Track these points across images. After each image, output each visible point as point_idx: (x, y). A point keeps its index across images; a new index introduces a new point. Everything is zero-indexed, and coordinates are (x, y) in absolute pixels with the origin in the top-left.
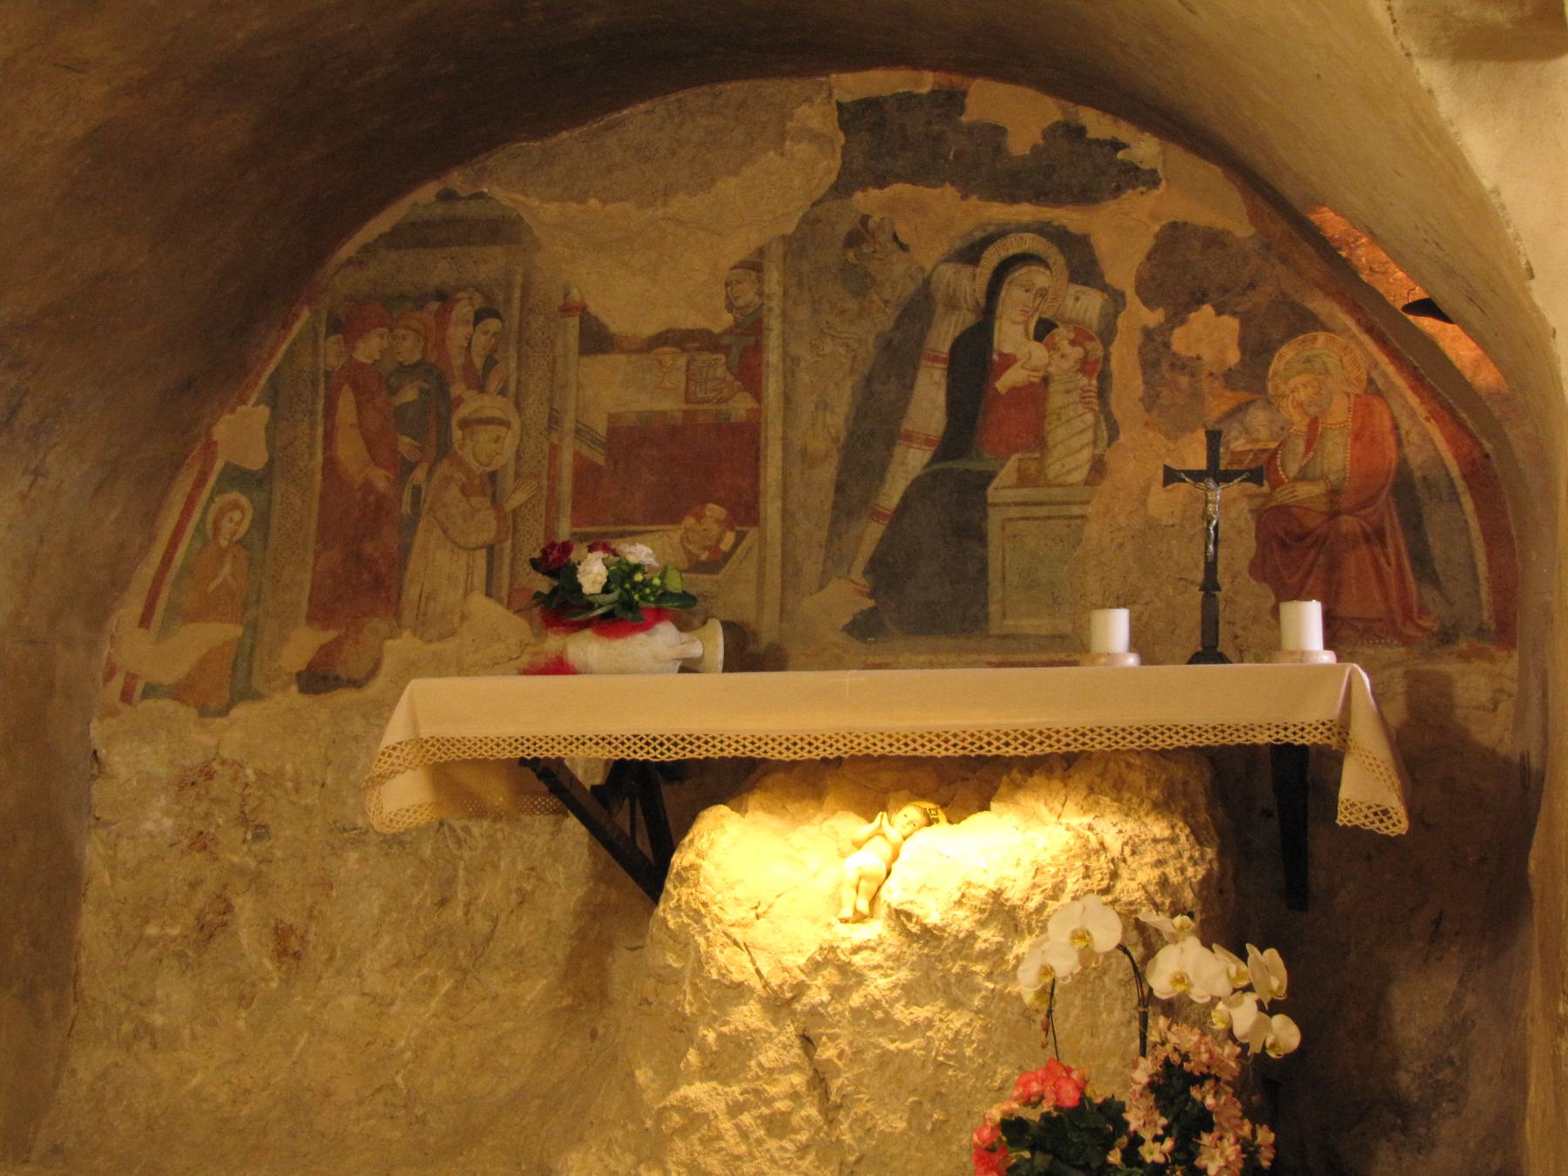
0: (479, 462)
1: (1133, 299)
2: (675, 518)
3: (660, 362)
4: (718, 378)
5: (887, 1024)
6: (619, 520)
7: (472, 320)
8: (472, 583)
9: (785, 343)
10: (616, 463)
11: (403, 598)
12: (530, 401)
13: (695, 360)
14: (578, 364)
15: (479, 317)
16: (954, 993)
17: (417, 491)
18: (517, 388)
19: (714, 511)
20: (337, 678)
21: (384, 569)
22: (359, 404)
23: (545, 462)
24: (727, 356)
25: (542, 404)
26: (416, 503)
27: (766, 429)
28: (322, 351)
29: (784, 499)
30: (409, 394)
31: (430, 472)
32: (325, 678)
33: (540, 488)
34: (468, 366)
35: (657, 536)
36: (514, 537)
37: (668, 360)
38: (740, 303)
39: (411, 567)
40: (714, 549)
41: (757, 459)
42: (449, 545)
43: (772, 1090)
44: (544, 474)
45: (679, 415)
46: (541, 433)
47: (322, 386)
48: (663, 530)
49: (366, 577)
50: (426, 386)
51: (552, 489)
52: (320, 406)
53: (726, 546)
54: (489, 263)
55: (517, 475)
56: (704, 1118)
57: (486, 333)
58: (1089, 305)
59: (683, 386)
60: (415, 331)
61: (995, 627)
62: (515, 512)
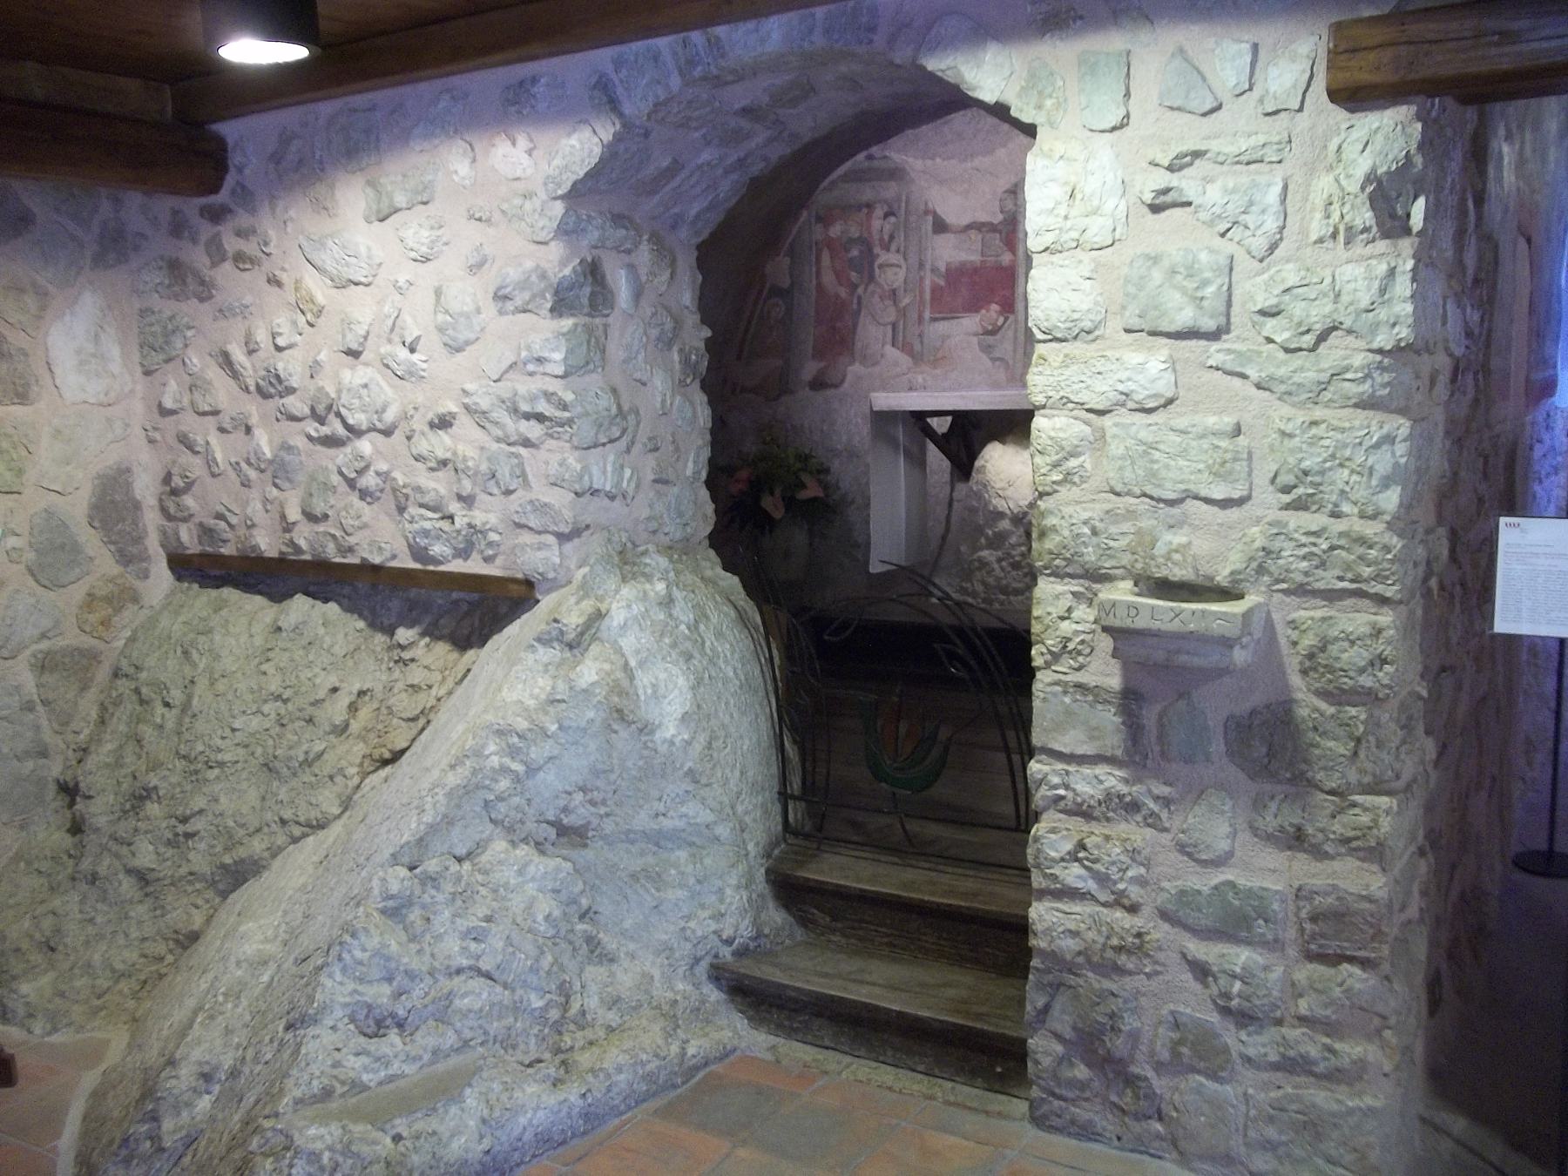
2: (977, 311)
6: (951, 311)
15: (886, 216)
19: (995, 307)
26: (859, 303)
30: (855, 253)
34: (881, 239)
43: (1014, 553)
53: (1000, 323)
54: (890, 190)
55: (905, 291)
56: (987, 564)
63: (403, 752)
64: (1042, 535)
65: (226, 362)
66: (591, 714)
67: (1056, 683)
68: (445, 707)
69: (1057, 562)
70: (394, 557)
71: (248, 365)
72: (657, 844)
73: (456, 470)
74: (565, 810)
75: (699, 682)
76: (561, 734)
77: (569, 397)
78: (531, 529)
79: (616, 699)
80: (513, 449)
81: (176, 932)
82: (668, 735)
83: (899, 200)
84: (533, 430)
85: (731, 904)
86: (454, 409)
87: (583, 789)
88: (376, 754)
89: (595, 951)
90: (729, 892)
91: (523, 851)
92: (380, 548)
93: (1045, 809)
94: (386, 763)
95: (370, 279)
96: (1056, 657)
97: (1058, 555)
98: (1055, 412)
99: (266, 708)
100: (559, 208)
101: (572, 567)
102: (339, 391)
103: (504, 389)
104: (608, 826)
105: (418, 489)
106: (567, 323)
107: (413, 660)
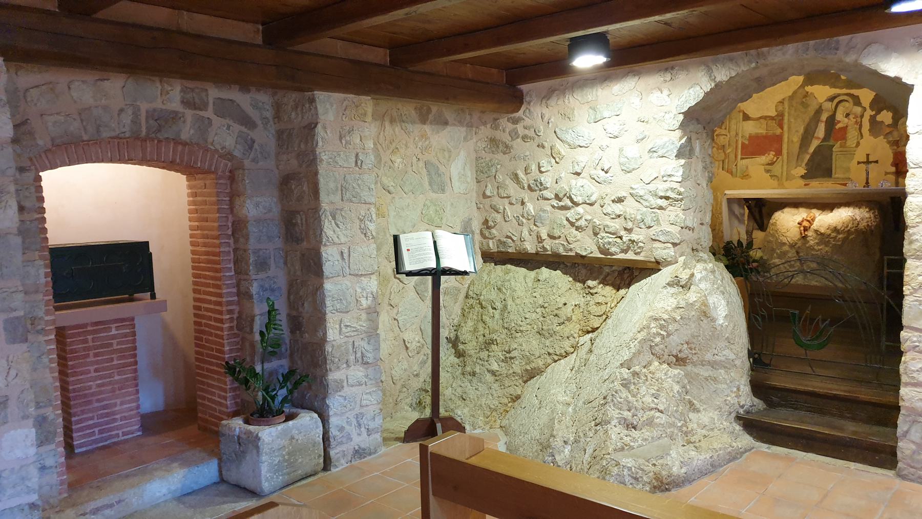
1: (868, 108)
5: (814, 249)
9: (789, 119)
16: (827, 244)
53: (774, 160)
58: (858, 110)
61: (833, 176)
63: (597, 328)
64: (911, 242)
65: (516, 177)
66: (693, 313)
67: (916, 301)
68: (616, 311)
69: (918, 253)
70: (592, 252)
71: (525, 179)
72: (712, 367)
73: (625, 219)
74: (680, 351)
75: (728, 302)
76: (681, 321)
77: (682, 190)
78: (660, 241)
79: (703, 308)
80: (652, 210)
81: (511, 395)
82: (721, 323)
84: (663, 203)
85: (743, 391)
86: (625, 195)
87: (687, 343)
88: (585, 329)
89: (692, 407)
90: (742, 387)
91: (665, 366)
92: (586, 249)
93: (909, 350)
94: (588, 332)
95: (588, 145)
96: (915, 290)
97: (918, 251)
98: (917, 195)
99: (538, 310)
100: (681, 117)
101: (678, 256)
102: (570, 190)
103: (652, 187)
104: (695, 358)
105: (607, 226)
106: (682, 161)
107: (596, 293)
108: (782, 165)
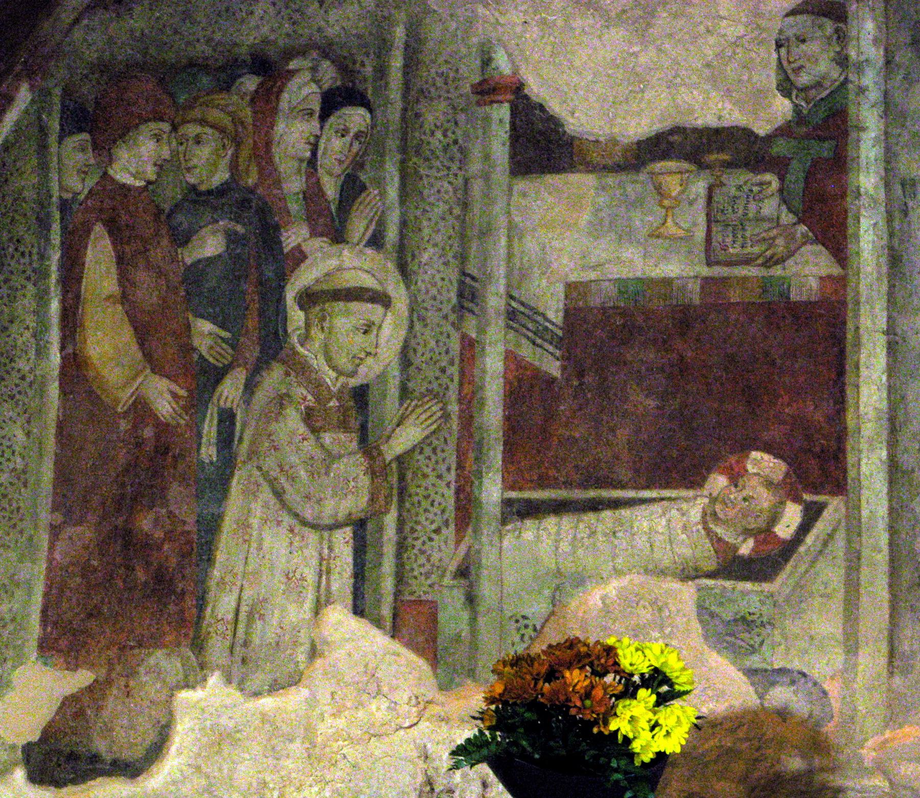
0: (334, 368)
3: (658, 189)
4: (769, 220)
7: (317, 107)
8: (328, 586)
9: (889, 157)
10: (581, 374)
11: (208, 612)
12: (425, 257)
13: (722, 184)
14: (510, 189)
17: (227, 418)
18: (402, 236)
20: (95, 758)
21: (173, 562)
22: (121, 260)
23: (454, 370)
24: (782, 179)
25: (446, 264)
26: (226, 440)
27: (857, 316)
28: (54, 163)
29: (892, 444)
31: (250, 387)
32: (73, 757)
33: (446, 416)
35: (657, 508)
36: (400, 507)
37: (673, 185)
38: (804, 79)
39: (220, 557)
40: (765, 534)
41: (841, 372)
42: (287, 520)
44: (453, 395)
45: (695, 287)
46: (445, 317)
47: (56, 227)
48: (670, 499)
49: (141, 575)
50: (240, 229)
51: (467, 420)
52: (55, 256)
53: (785, 529)
55: (405, 392)
57: (344, 133)
59: (700, 234)
60: (222, 130)
62: (399, 459)
83: (383, 47)
108: (852, 585)
